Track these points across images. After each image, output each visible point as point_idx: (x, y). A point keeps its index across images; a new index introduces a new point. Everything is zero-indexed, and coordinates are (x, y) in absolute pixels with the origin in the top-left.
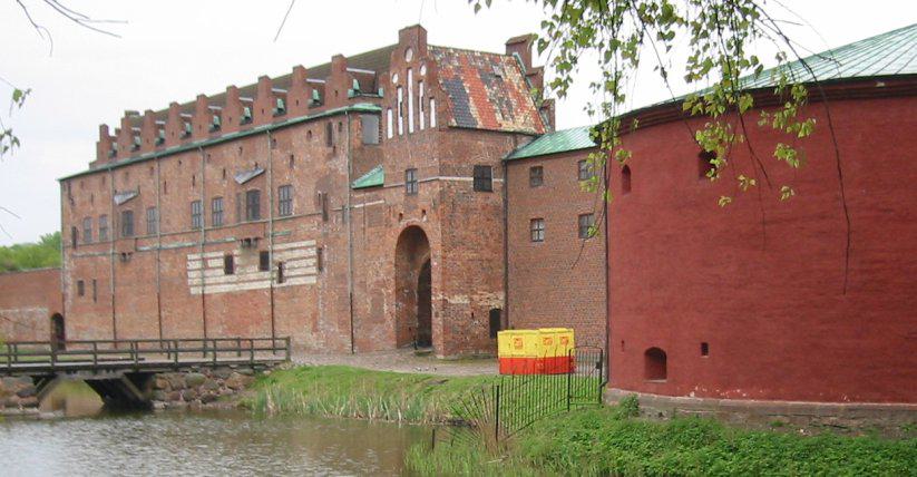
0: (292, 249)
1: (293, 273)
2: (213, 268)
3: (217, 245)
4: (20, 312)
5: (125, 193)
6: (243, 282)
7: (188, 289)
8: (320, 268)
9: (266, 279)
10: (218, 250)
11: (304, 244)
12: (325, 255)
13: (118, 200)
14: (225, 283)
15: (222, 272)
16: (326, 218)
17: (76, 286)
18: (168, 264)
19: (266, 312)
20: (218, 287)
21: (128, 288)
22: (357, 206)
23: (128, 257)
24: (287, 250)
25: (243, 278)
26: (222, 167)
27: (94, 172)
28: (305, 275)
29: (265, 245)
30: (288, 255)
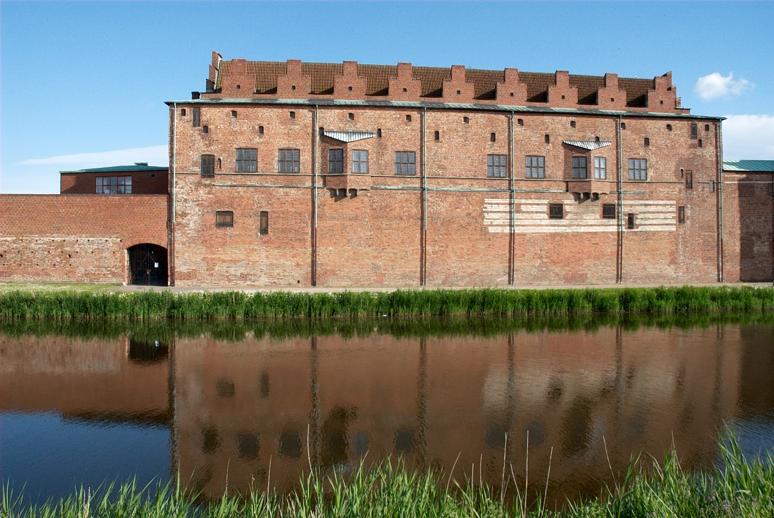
0: (646, 205)
1: (646, 222)
2: (528, 212)
3: (539, 194)
4: (14, 242)
7: (484, 230)
8: (681, 220)
10: (539, 198)
11: (661, 202)
12: (688, 212)
14: (547, 226)
15: (546, 216)
16: (689, 186)
17: (212, 219)
19: (612, 248)
21: (347, 223)
24: (641, 205)
30: (643, 209)
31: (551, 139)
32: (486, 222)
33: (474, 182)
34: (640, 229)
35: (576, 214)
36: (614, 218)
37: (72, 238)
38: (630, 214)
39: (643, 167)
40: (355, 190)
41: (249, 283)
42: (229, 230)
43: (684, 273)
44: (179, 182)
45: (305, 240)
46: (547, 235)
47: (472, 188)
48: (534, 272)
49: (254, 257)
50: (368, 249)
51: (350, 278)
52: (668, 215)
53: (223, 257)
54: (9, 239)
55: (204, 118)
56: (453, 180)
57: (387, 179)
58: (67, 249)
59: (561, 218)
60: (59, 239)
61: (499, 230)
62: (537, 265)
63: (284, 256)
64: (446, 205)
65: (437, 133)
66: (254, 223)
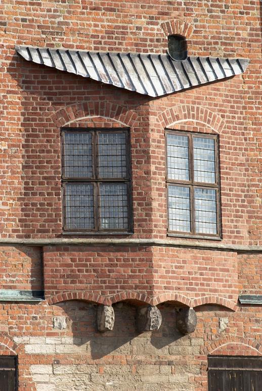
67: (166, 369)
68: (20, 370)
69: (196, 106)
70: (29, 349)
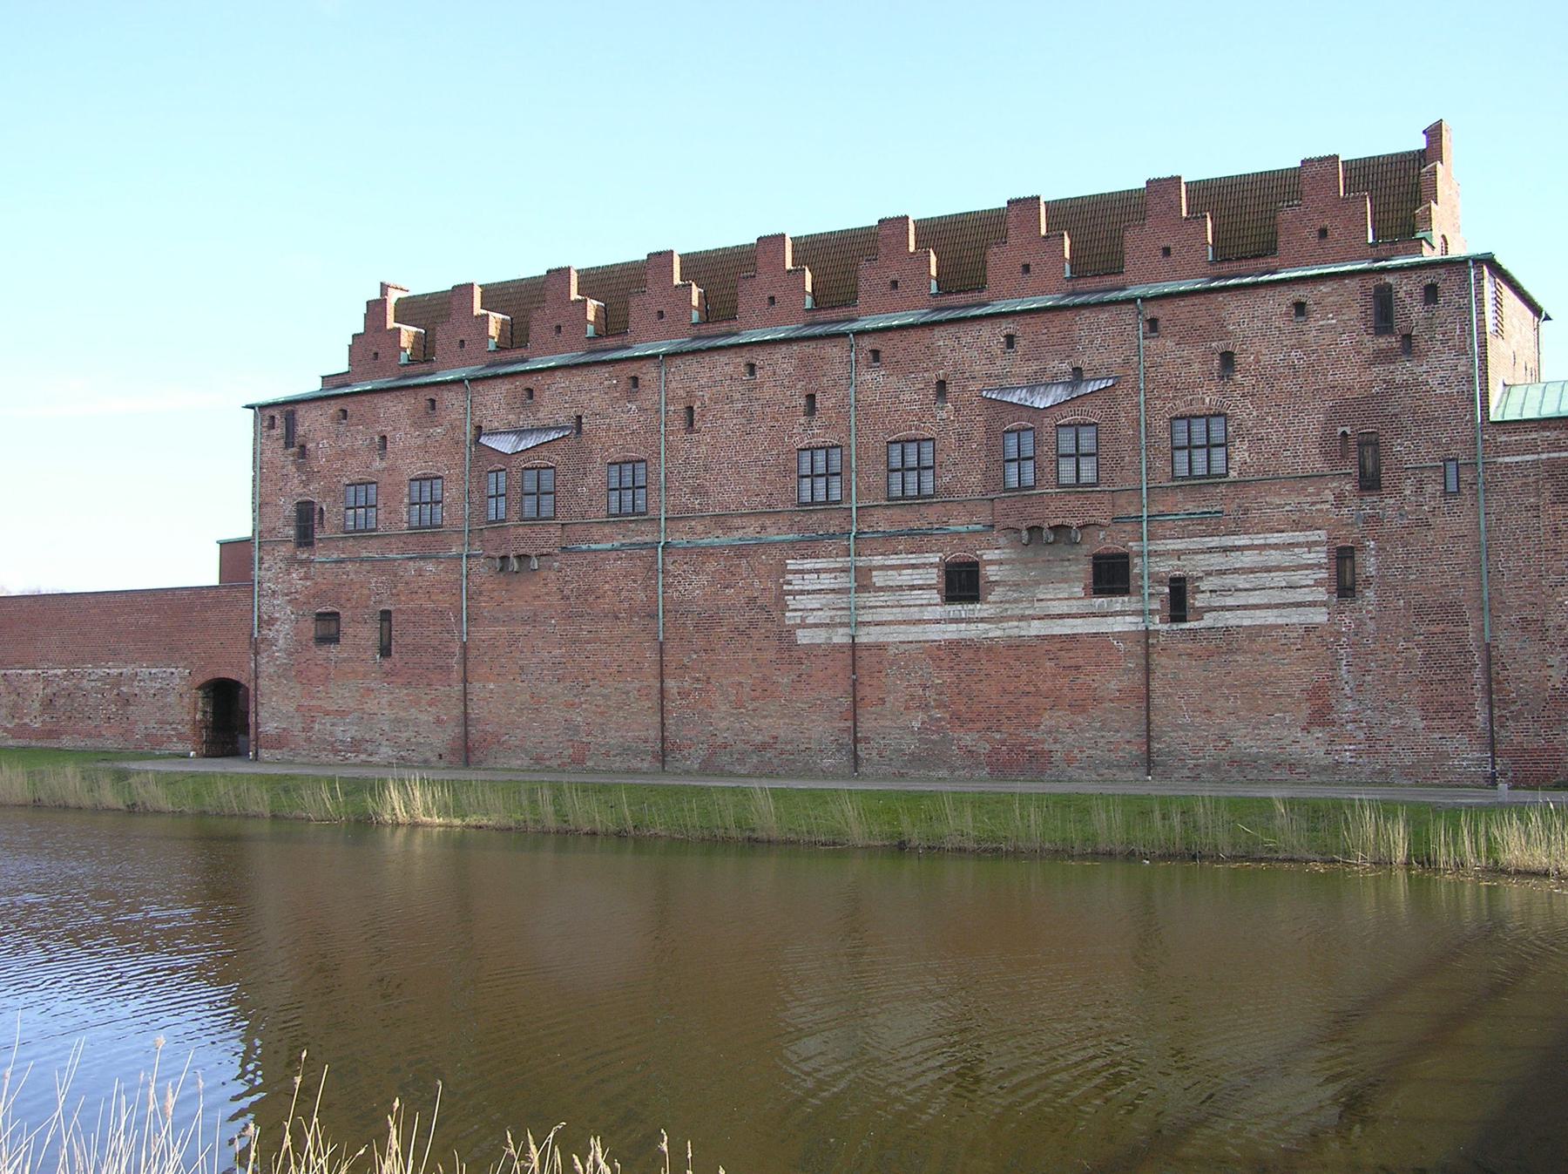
0: (1226, 550)
1: (1230, 601)
3: (917, 538)
4: (65, 677)
5: (520, 433)
6: (1022, 618)
7: (785, 638)
8: (1345, 587)
9: (1123, 613)
11: (1275, 538)
12: (1369, 564)
13: (505, 444)
14: (938, 622)
15: (935, 597)
16: (1369, 483)
17: (310, 628)
18: (704, 579)
20: (913, 629)
21: (520, 630)
22: (1507, 459)
23: (535, 564)
24: (1210, 550)
25: (1016, 610)
26: (932, 376)
27: (335, 392)
28: (1277, 606)
29: (1105, 542)
30: (1217, 561)
31: (951, 389)
32: (791, 618)
33: (768, 523)
34: (1208, 620)
35: (1016, 586)
36: (1125, 591)
37: (128, 670)
38: (1173, 580)
39: (1217, 435)
40: (527, 557)
41: (363, 757)
42: (333, 649)
43: (1359, 754)
44: (266, 558)
45: (449, 668)
46: (939, 646)
47: (763, 535)
48: (911, 745)
49: (371, 706)
50: (559, 688)
51: (526, 752)
52: (1297, 577)
53: (326, 705)
54: (59, 672)
55: (300, 430)
56: (721, 520)
57: (594, 530)
58: (124, 689)
59: (974, 598)
60: (115, 671)
61: (820, 636)
62: (916, 725)
63: (417, 703)
64: (704, 579)
65: (690, 409)
66: (369, 634)
67: (1067, 563)
68: (980, 569)
69: (1080, 409)
70: (985, 557)
